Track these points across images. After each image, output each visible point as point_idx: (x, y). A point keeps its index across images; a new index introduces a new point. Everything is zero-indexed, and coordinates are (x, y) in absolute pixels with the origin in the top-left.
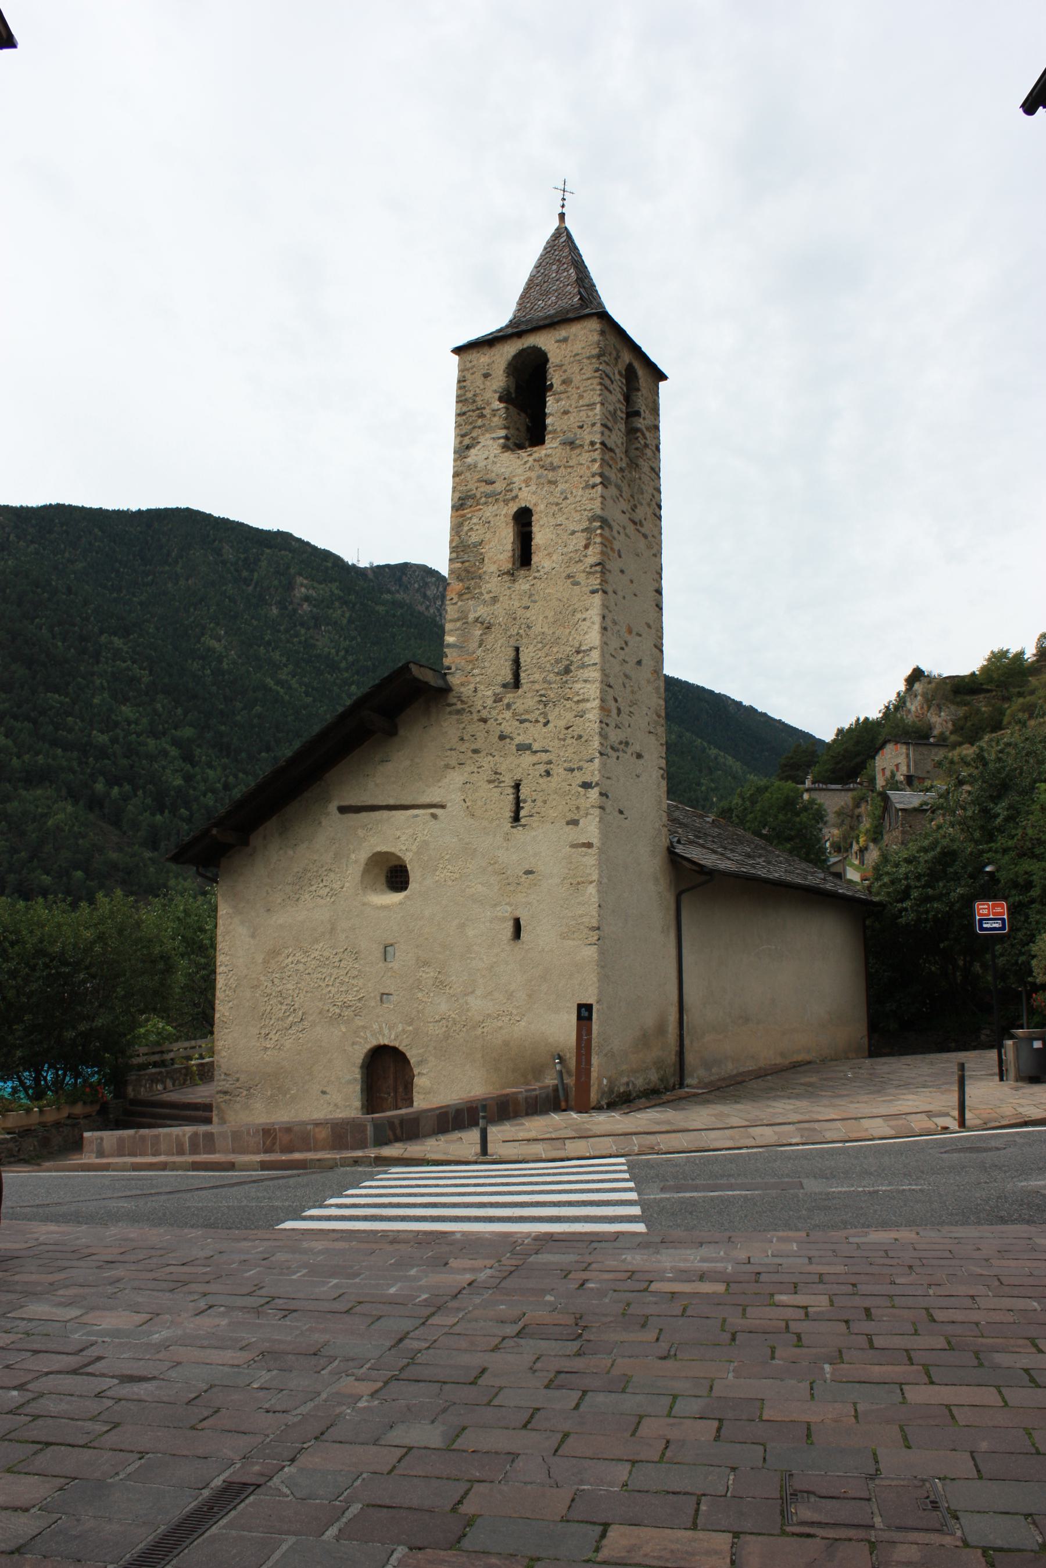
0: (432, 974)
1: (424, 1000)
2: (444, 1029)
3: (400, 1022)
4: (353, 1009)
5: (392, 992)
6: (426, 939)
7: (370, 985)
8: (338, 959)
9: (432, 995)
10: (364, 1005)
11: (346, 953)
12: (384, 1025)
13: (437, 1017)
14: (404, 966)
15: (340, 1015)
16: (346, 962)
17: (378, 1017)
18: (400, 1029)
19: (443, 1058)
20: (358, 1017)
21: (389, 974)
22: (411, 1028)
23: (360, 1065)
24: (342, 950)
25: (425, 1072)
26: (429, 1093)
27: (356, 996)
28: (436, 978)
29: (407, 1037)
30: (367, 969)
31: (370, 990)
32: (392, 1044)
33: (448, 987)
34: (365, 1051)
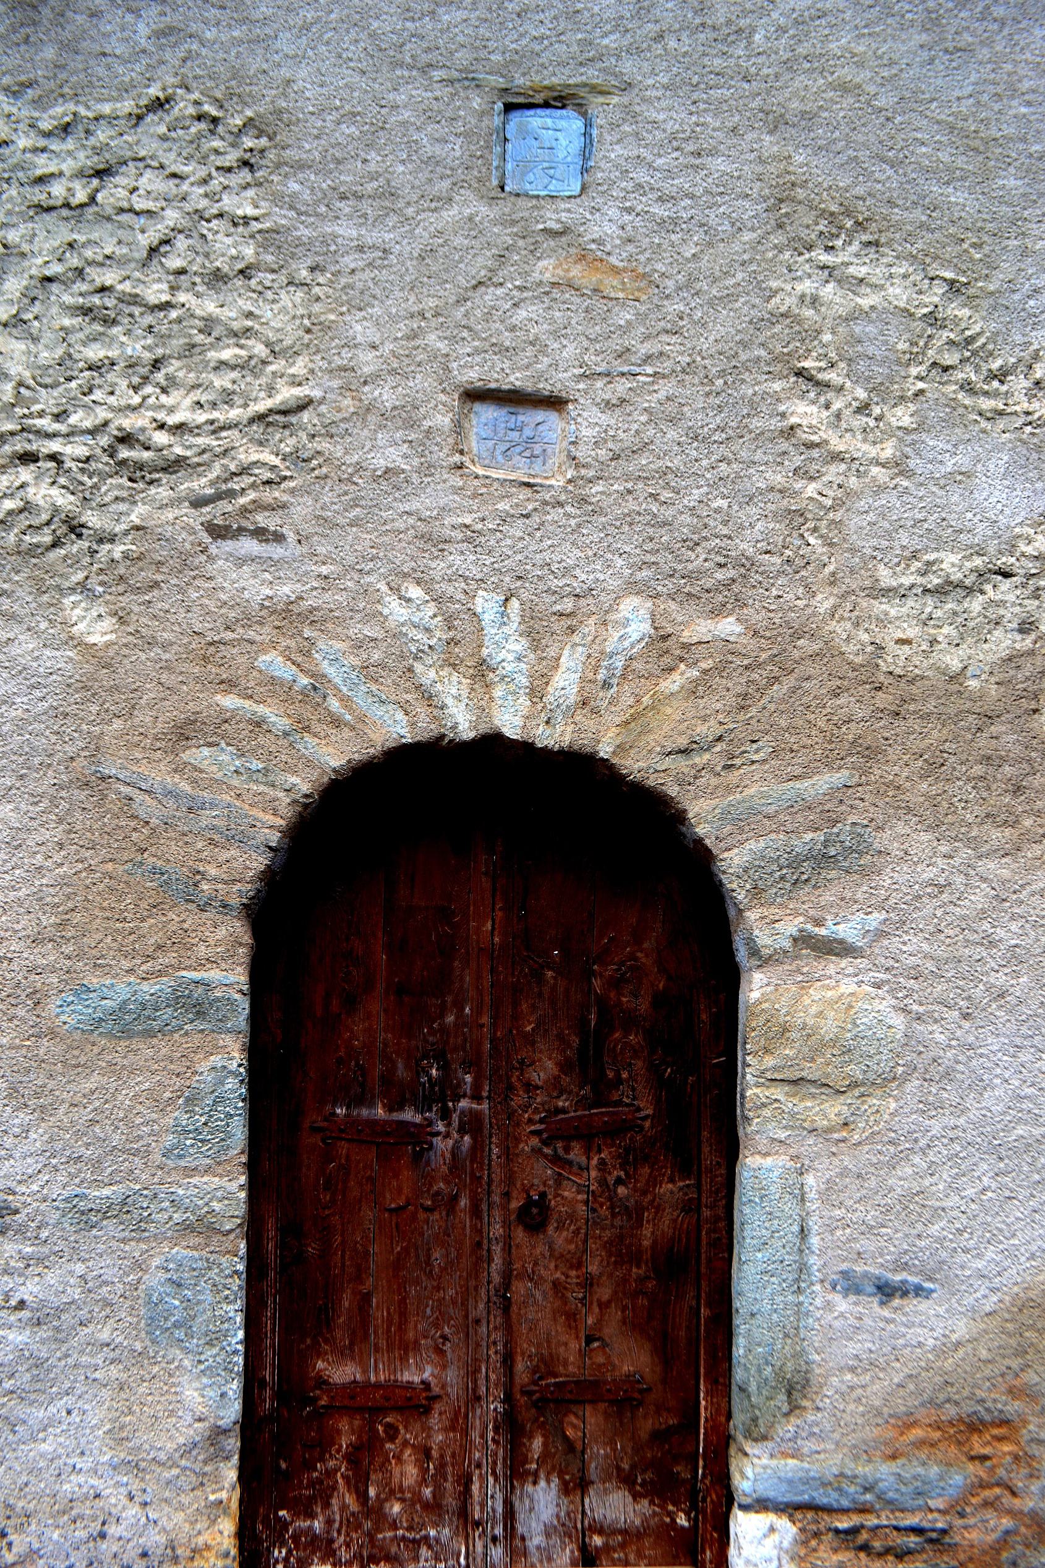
0: (899, 294)
1: (837, 444)
2: (1004, 642)
3: (633, 587)
4: (201, 485)
5: (559, 381)
6: (844, 88)
7: (360, 330)
8: (84, 159)
9: (902, 416)
10: (297, 458)
11: (157, 125)
12: (486, 604)
13: (951, 563)
14: (669, 225)
15: (76, 529)
16: (150, 181)
17: (438, 544)
18: (639, 628)
19: (997, 836)
20: (249, 546)
21: (546, 268)
22: (728, 626)
23: (239, 892)
24: (127, 106)
25: (847, 930)
26: (886, 1082)
27: (227, 398)
28: (933, 319)
29: (692, 691)
30: (346, 230)
31: (368, 363)
32: (548, 737)
33: (1019, 384)
34: (303, 784)
